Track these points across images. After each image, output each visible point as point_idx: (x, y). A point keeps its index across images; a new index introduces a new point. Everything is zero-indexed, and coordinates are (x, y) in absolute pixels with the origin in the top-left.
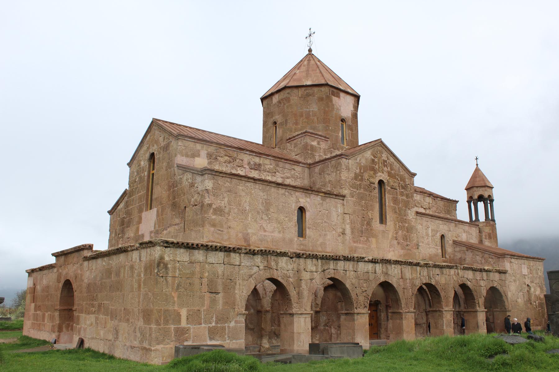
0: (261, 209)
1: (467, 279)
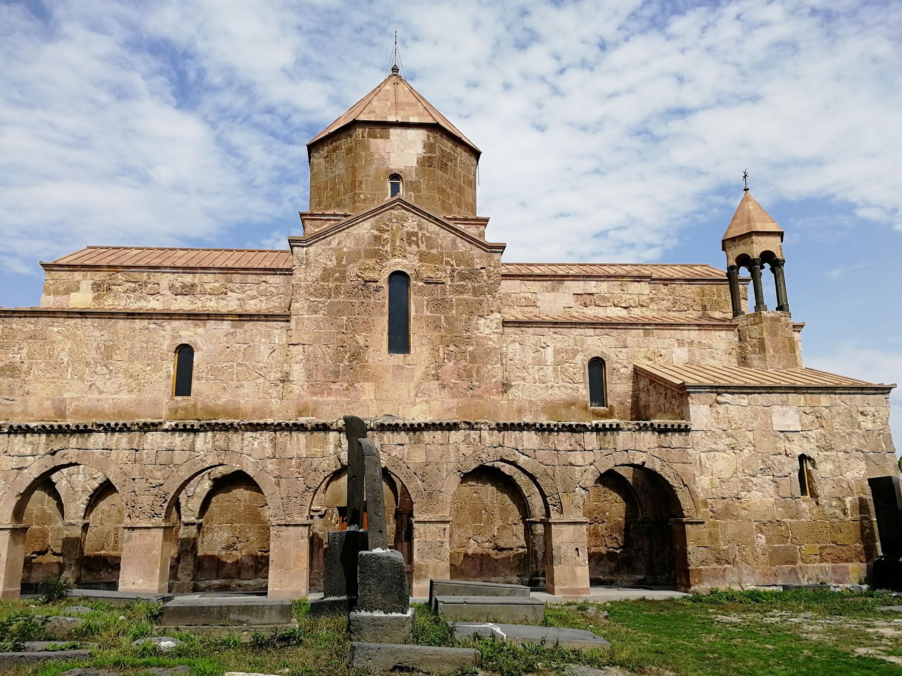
0: (94, 358)
1: (517, 450)
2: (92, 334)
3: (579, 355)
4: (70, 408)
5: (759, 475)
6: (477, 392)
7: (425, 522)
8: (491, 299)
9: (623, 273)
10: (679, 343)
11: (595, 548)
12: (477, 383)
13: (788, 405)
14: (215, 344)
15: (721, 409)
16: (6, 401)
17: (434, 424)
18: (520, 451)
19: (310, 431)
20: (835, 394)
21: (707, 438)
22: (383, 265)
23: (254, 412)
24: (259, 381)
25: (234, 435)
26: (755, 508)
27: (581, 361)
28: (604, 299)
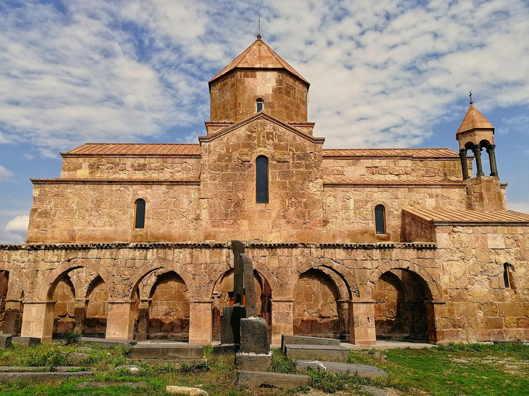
0: (90, 206)
1: (333, 260)
2: (89, 193)
3: (369, 203)
4: (78, 235)
5: (479, 275)
6: (308, 225)
7: (278, 301)
8: (317, 171)
9: (396, 154)
10: (430, 196)
11: (379, 317)
12: (308, 221)
13: (497, 233)
14: (158, 198)
15: (455, 235)
16: (42, 231)
17: (283, 245)
18: (334, 260)
19: (212, 248)
20: (527, 226)
21: (446, 253)
22: (253, 152)
23: (180, 237)
24: (182, 219)
25: (169, 251)
26: (476, 295)
27: (370, 207)
28: (384, 170)
